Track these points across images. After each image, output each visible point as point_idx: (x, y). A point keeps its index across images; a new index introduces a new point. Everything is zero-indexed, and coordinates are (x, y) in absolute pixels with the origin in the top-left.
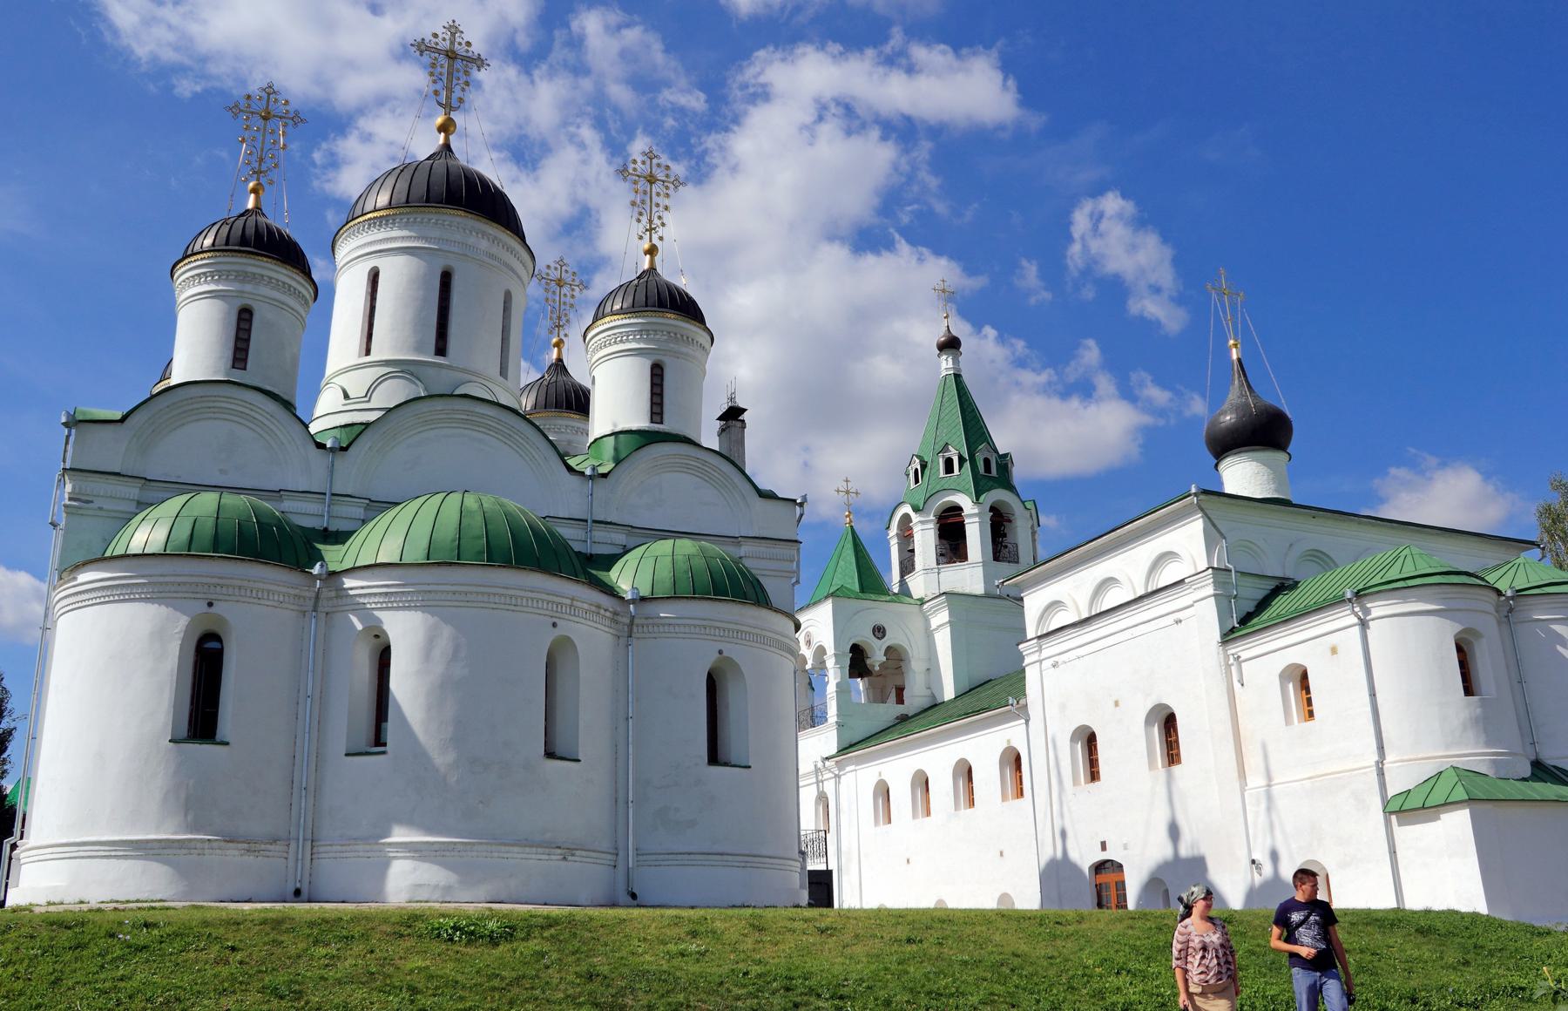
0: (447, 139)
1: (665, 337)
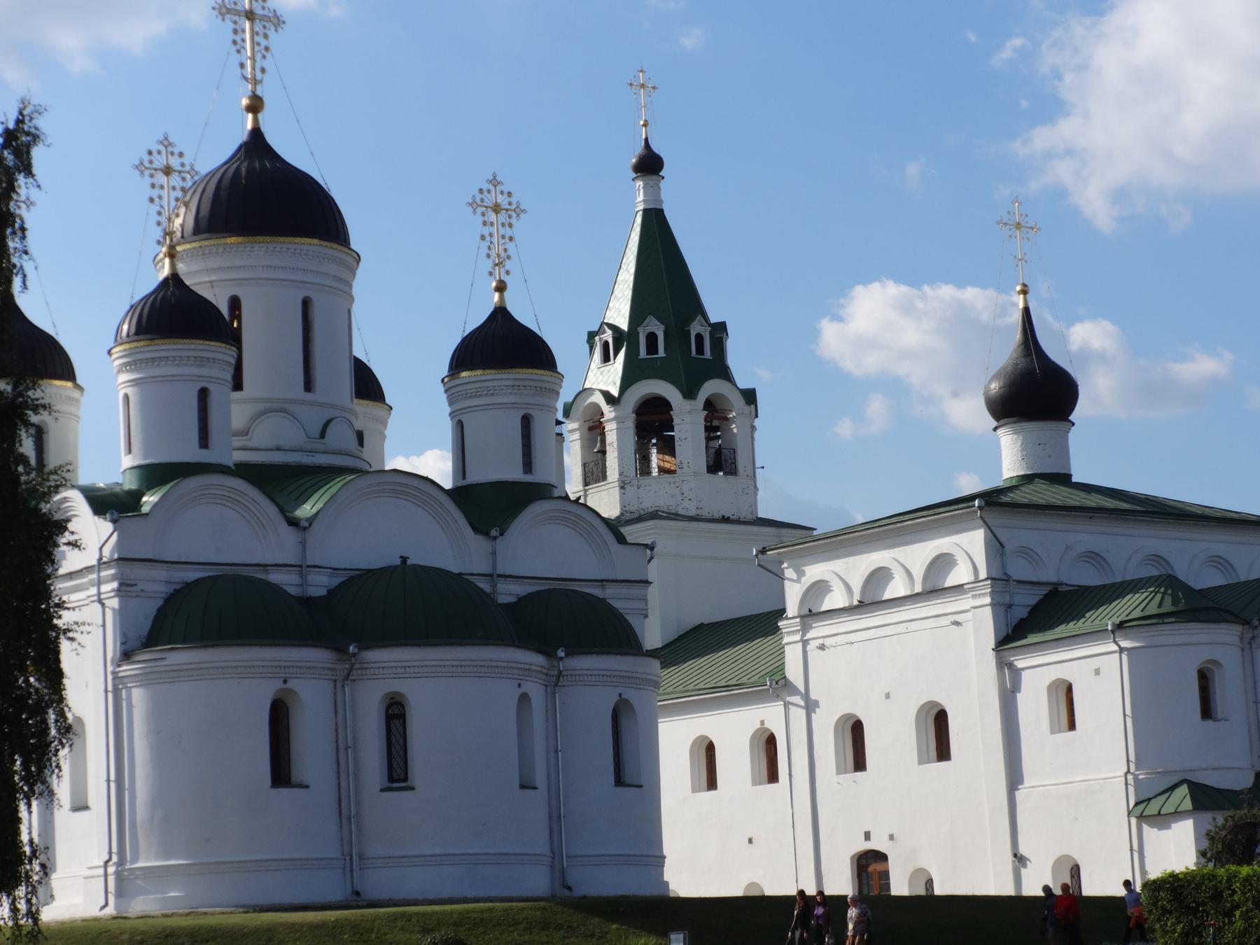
0: (256, 120)
1: (532, 392)
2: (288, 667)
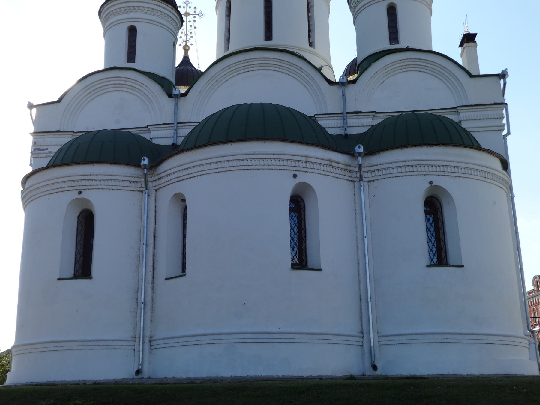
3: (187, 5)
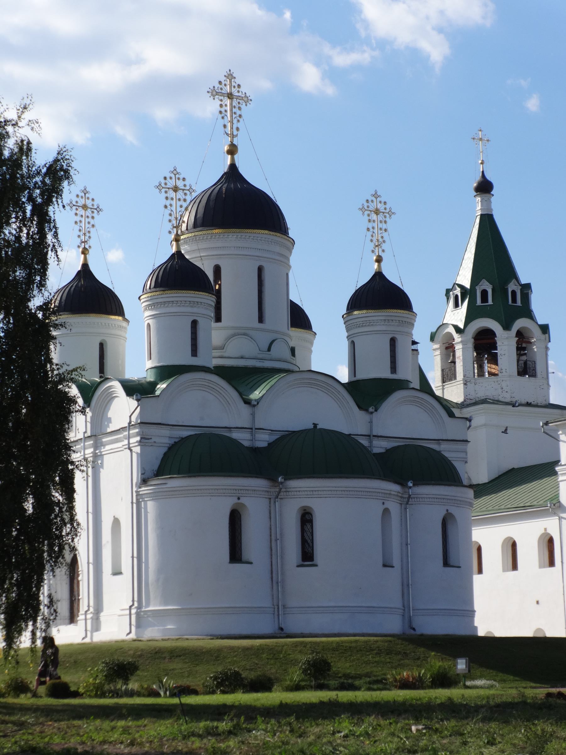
0: (233, 159)
2: (241, 490)
3: (85, 194)
